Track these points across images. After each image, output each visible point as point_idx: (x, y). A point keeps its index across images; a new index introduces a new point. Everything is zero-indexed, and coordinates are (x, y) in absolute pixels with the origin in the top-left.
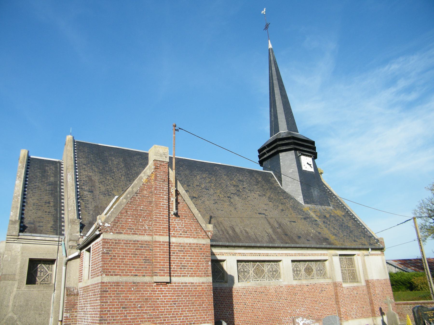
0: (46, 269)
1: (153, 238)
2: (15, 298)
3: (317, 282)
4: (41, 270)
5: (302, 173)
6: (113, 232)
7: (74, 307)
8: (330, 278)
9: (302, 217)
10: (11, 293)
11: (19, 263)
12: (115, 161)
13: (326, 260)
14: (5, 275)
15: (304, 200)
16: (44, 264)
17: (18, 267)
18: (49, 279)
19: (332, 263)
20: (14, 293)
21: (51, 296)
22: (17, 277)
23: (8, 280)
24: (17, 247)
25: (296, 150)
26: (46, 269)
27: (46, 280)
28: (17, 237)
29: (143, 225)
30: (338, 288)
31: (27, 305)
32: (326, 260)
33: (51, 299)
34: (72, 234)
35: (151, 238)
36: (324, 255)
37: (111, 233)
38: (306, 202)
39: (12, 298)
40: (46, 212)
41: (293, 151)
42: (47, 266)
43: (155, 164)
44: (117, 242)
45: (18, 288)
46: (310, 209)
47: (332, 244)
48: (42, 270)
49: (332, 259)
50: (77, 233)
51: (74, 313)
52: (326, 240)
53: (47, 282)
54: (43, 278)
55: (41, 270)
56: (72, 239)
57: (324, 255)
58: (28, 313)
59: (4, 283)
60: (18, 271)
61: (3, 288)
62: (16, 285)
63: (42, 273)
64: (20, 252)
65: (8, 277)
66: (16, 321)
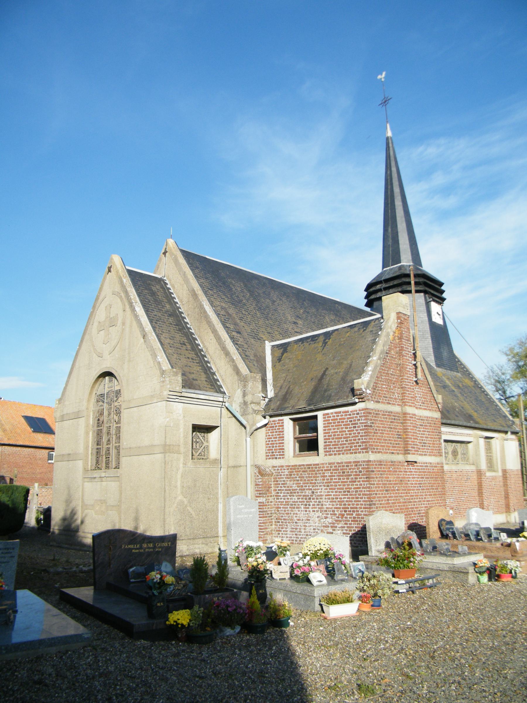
0: (201, 438)
1: (402, 410)
2: (182, 477)
3: (463, 468)
4: (196, 440)
5: (433, 325)
6: (373, 400)
7: (268, 491)
8: (473, 464)
9: (440, 384)
10: (177, 470)
11: (182, 430)
12: (238, 287)
13: (469, 442)
14: (170, 445)
15: (436, 362)
16: (199, 432)
17: (182, 435)
18: (206, 453)
19: (477, 445)
20: (181, 471)
21: (218, 476)
22: (182, 449)
23: (173, 452)
24: (178, 407)
25: (425, 292)
26: (201, 438)
27: (203, 453)
28: (179, 394)
29: (394, 393)
30: (483, 477)
31: (195, 486)
32: (469, 442)
33: (218, 479)
34: (254, 395)
35: (400, 409)
36: (469, 435)
37: (372, 402)
38: (438, 366)
39: (179, 476)
40: (188, 358)
41: (422, 294)
42: (203, 434)
43: (398, 318)
44: (377, 413)
45: (185, 464)
46: (444, 375)
47: (476, 423)
48: (198, 440)
49: (478, 441)
50: (259, 393)
51: (269, 498)
52: (470, 417)
53: (203, 457)
54: (200, 451)
55: (196, 440)
56: (254, 401)
57: (469, 435)
58: (197, 496)
59: (169, 456)
60: (182, 440)
61: (169, 463)
62: (182, 460)
63: (198, 444)
64: (182, 415)
65: (173, 449)
66: (186, 506)
